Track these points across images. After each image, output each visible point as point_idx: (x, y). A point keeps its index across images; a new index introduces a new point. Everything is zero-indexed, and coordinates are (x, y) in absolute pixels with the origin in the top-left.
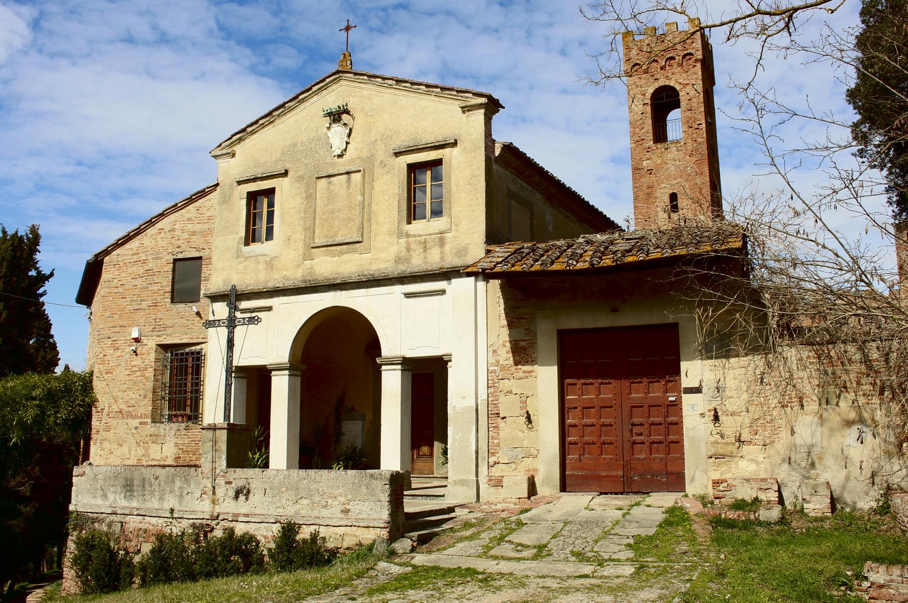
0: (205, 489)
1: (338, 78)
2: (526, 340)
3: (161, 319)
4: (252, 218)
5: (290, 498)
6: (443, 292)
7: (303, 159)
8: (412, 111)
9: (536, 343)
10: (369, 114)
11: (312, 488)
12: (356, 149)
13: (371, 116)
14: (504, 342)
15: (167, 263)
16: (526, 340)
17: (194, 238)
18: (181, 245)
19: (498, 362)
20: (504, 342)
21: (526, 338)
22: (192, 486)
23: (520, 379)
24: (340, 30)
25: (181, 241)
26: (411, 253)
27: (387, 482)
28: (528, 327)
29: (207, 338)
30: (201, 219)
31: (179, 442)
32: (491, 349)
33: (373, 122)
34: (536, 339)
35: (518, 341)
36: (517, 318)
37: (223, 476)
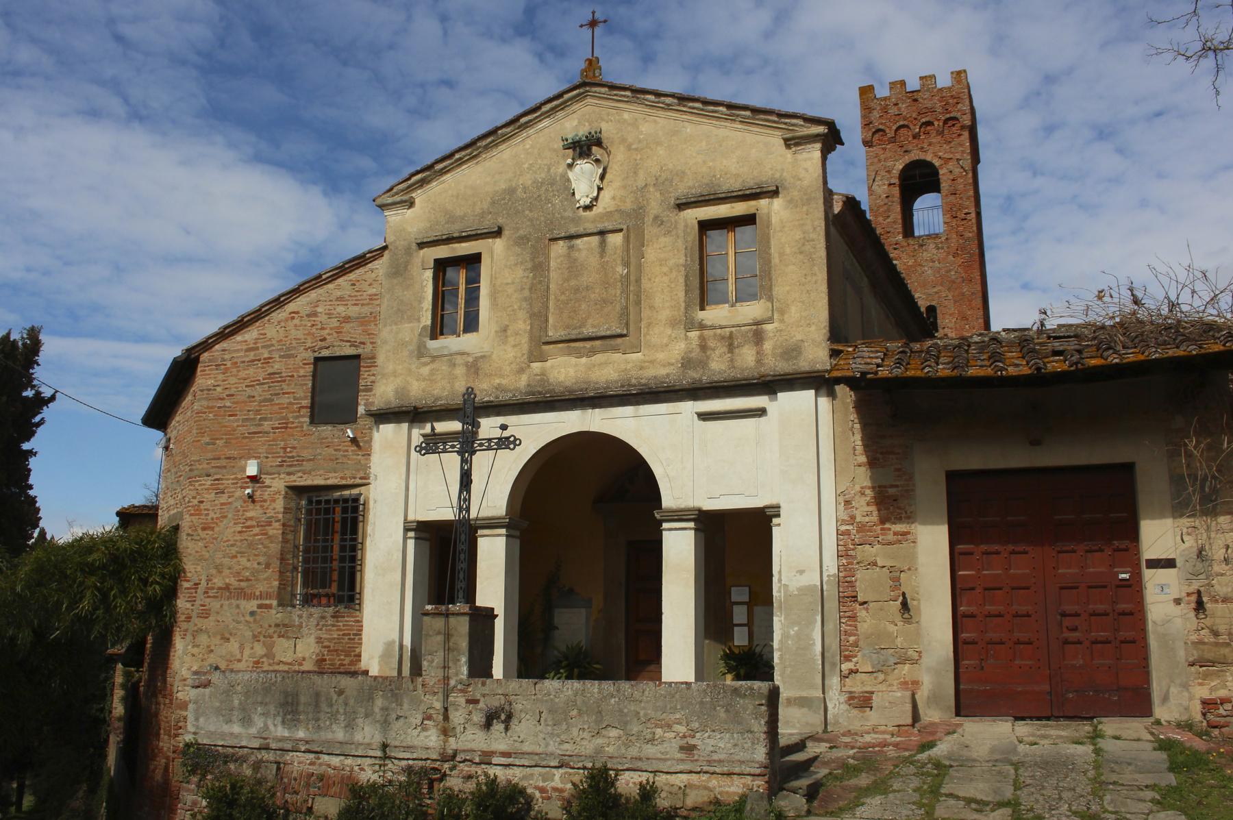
0: (432, 711)
1: (583, 93)
2: (897, 486)
3: (294, 448)
4: (441, 298)
5: (586, 727)
6: (762, 412)
7: (527, 212)
8: (704, 144)
9: (913, 490)
10: (633, 147)
11: (626, 711)
12: (614, 198)
13: (636, 149)
14: (862, 488)
15: (305, 364)
16: (897, 486)
17: (347, 327)
18: (328, 337)
19: (853, 517)
20: (862, 488)
21: (898, 483)
22: (406, 706)
23: (890, 544)
24: (581, 26)
25: (327, 331)
26: (708, 353)
27: (764, 702)
28: (899, 466)
29: (369, 478)
30: (359, 298)
31: (324, 636)
32: (841, 499)
33: (640, 159)
34: (914, 485)
35: (885, 487)
36: (881, 453)
37: (462, 691)
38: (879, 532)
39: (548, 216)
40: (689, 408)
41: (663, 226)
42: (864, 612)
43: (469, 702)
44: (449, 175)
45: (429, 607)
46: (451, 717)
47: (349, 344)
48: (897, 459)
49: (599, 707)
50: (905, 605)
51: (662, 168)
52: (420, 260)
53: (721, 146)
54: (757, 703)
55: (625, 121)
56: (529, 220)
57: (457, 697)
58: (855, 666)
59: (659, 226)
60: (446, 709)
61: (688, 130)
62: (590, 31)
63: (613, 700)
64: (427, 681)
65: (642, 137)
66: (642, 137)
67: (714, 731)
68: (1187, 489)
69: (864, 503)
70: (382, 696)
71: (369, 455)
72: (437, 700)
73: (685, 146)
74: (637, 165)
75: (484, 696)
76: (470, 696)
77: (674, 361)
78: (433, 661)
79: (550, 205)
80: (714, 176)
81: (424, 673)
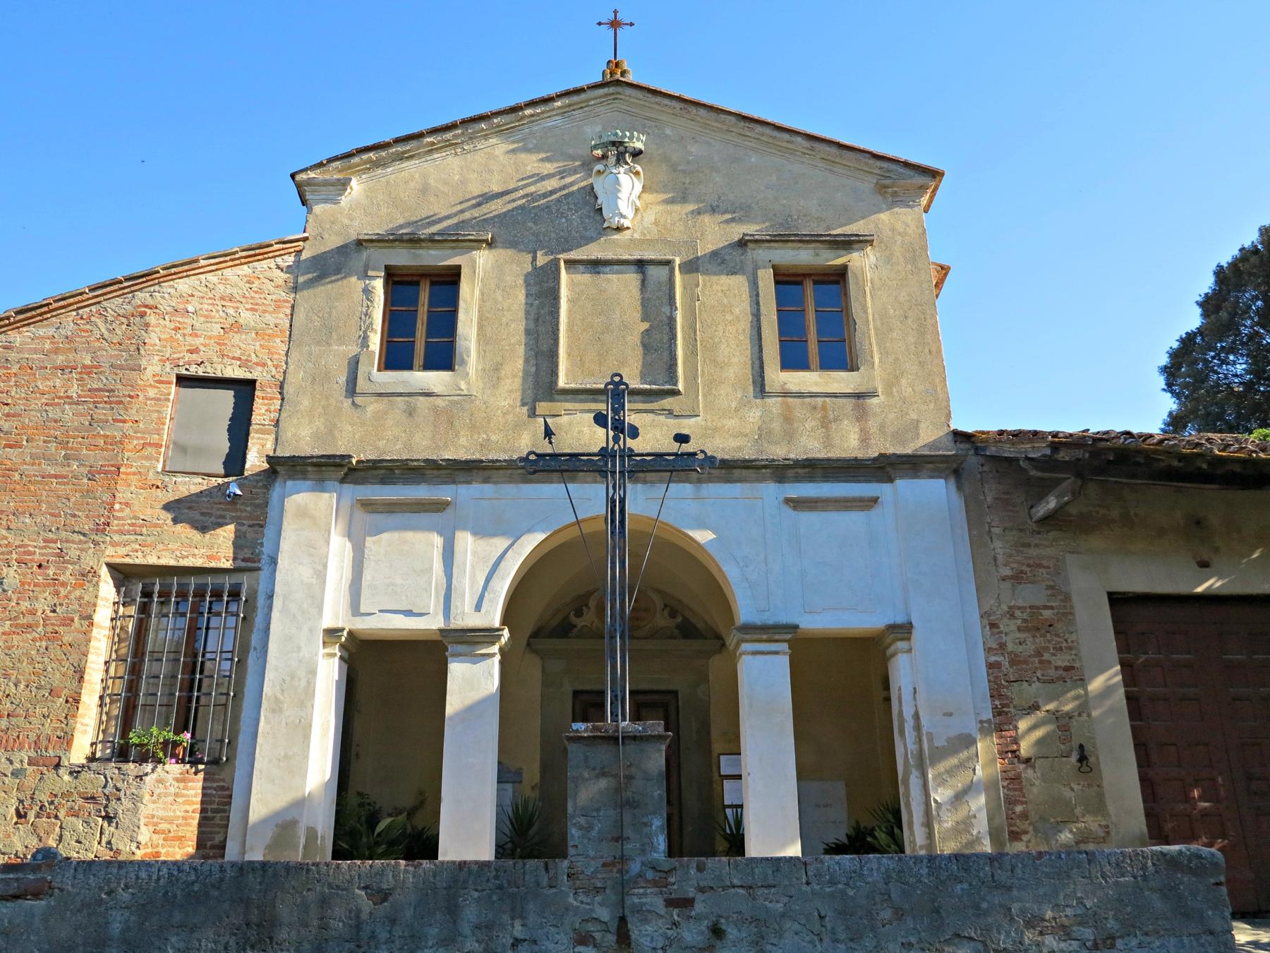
0: (591, 927)
1: (612, 94)
2: (1052, 608)
3: (127, 504)
5: (913, 940)
6: (870, 503)
7: (530, 224)
8: (774, 178)
9: (1072, 614)
10: (680, 168)
11: (984, 905)
12: (656, 223)
13: (684, 172)
14: (1010, 607)
15: (157, 382)
16: (1052, 608)
17: (236, 338)
18: (202, 348)
19: (1002, 646)
20: (1010, 607)
21: (1053, 604)
22: (532, 919)
23: (1052, 681)
24: (600, 24)
25: (201, 340)
26: (795, 425)
27: (1222, 879)
28: (1052, 584)
29: (259, 561)
30: (259, 301)
32: (986, 622)
33: (690, 183)
34: (1072, 607)
35: (1038, 608)
36: (1029, 565)
37: (655, 883)
38: (1037, 665)
39: (562, 234)
40: (771, 492)
41: (724, 266)
42: (1030, 771)
43: (671, 903)
44: (412, 162)
45: (580, 726)
46: (634, 934)
47: (238, 363)
48: (1047, 574)
49: (934, 901)
50: (1083, 758)
51: (720, 198)
52: (362, 264)
53: (797, 183)
54: (1212, 881)
55: (667, 136)
56: (533, 234)
57: (645, 894)
58: (1027, 847)
59: (719, 264)
60: (623, 920)
61: (753, 160)
62: (612, 32)
63: (959, 887)
64: (580, 863)
65: (691, 158)
66: (691, 158)
67: (1147, 934)
68: (1073, 675)
69: (1014, 628)
70: (478, 900)
71: (262, 526)
72: (601, 904)
73: (749, 177)
74: (686, 189)
75: (701, 890)
76: (676, 891)
77: (748, 431)
78: (590, 828)
79: (563, 220)
80: (791, 216)
81: (571, 851)
